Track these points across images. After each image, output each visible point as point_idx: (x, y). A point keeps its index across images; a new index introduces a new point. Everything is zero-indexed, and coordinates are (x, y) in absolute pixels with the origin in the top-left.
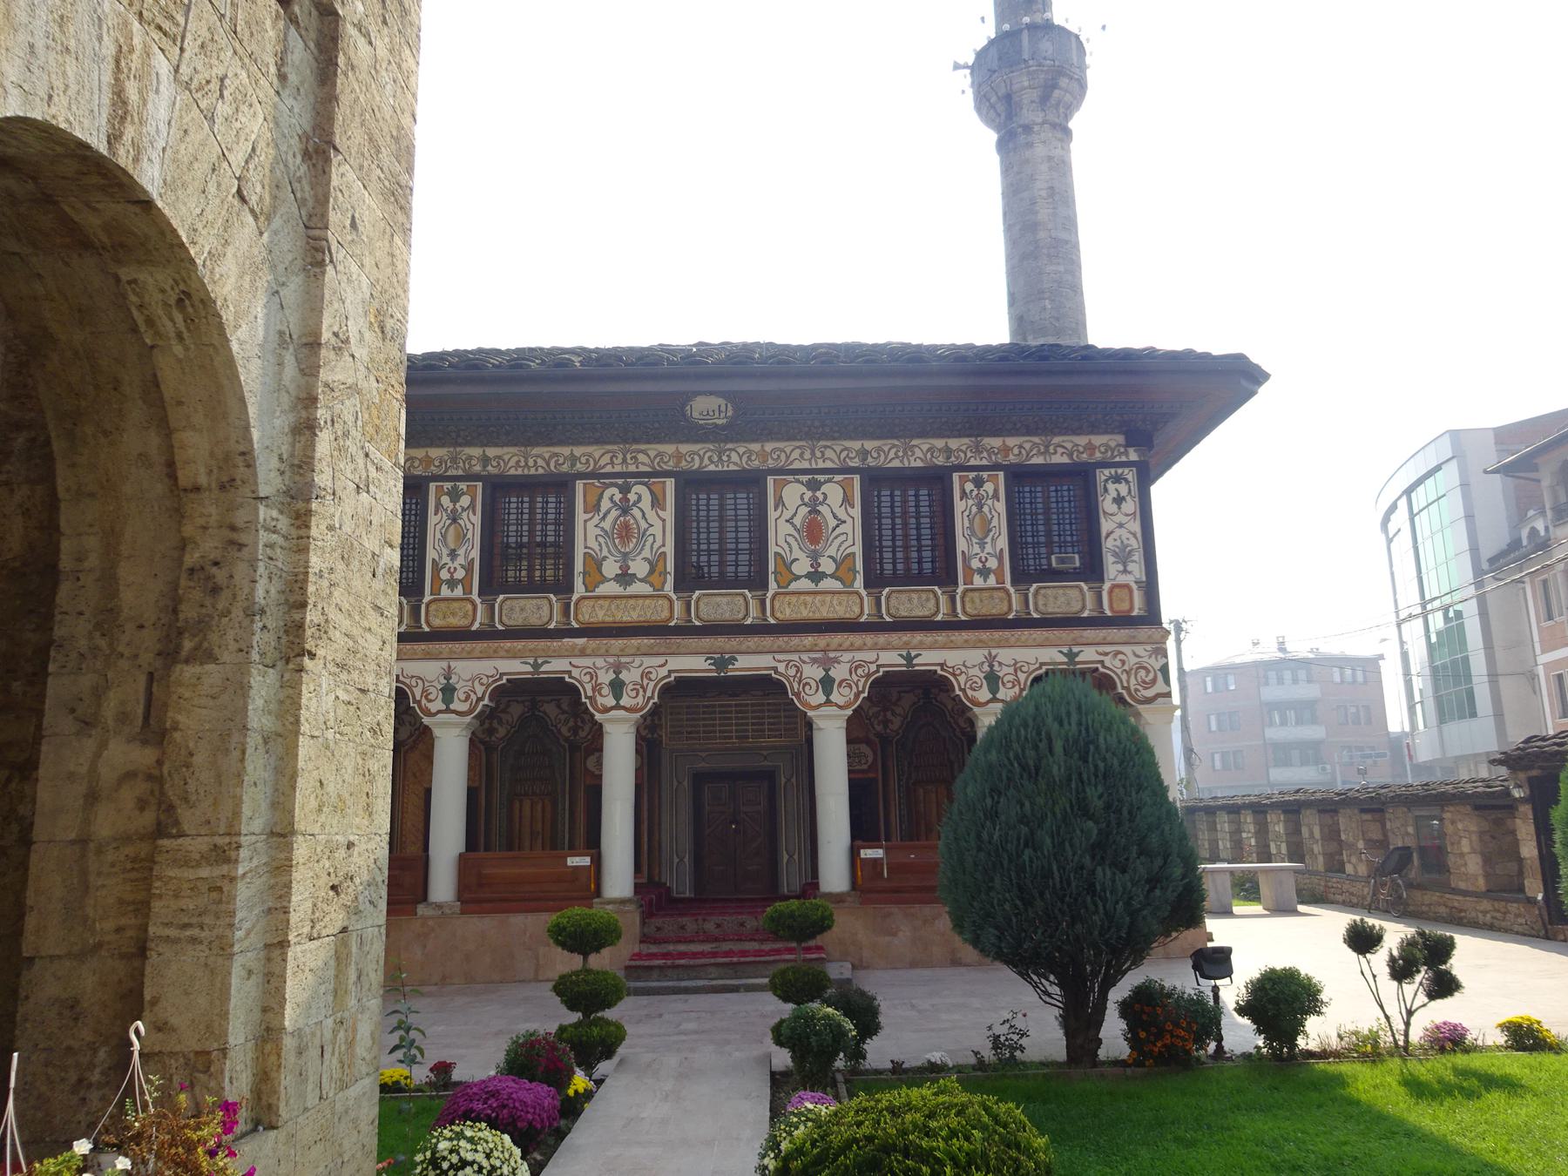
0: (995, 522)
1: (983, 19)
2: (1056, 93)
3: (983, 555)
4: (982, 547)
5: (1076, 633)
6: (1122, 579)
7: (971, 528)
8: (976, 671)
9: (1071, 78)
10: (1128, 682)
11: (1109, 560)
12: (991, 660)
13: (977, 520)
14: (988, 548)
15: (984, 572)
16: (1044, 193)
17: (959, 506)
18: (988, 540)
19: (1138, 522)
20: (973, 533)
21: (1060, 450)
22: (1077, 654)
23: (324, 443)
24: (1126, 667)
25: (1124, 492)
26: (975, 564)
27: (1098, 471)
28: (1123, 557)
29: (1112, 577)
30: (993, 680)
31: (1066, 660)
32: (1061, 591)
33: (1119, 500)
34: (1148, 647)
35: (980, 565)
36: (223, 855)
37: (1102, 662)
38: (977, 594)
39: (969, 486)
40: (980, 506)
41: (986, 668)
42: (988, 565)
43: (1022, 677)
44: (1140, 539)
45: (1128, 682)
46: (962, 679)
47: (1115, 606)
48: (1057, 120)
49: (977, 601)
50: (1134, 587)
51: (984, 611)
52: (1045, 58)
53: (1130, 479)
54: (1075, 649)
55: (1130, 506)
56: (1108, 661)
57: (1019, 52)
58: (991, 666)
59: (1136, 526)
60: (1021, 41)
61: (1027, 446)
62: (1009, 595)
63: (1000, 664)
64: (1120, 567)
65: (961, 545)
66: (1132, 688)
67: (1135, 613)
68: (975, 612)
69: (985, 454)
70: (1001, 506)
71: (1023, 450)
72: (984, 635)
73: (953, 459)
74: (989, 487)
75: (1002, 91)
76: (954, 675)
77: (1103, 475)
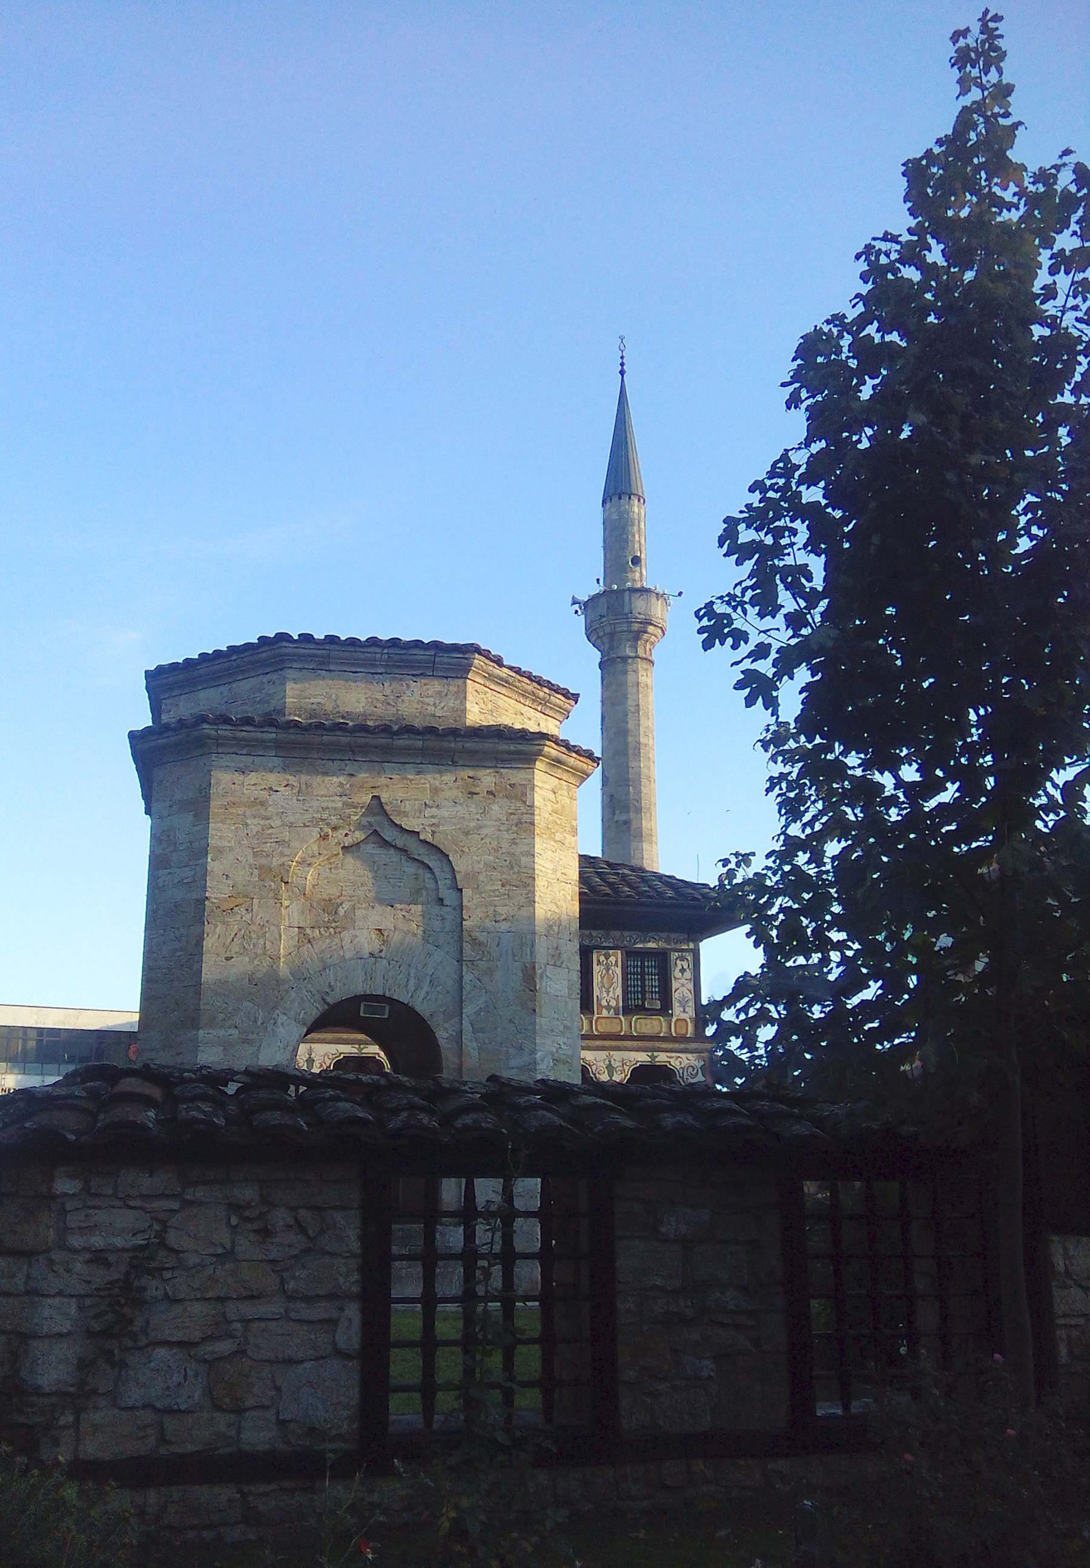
0: (615, 980)
1: (598, 580)
2: (645, 636)
3: (608, 998)
4: (608, 992)
5: (657, 1044)
6: (683, 1016)
7: (602, 982)
8: (601, 1064)
9: (655, 626)
10: (683, 1073)
11: (676, 1004)
12: (609, 1057)
13: (605, 979)
14: (611, 994)
15: (608, 1008)
16: (632, 709)
17: (596, 968)
18: (611, 990)
19: (692, 983)
20: (603, 986)
21: (653, 940)
22: (656, 1057)
24: (682, 1066)
25: (686, 967)
26: (604, 1003)
27: (672, 953)
28: (683, 1004)
29: (677, 1014)
30: (610, 1068)
31: (650, 1060)
32: (649, 1021)
33: (683, 970)
34: (694, 1055)
35: (606, 1004)
37: (669, 1062)
38: (603, 1020)
39: (602, 958)
40: (608, 970)
41: (607, 1062)
42: (610, 1004)
43: (626, 1068)
44: (692, 992)
45: (683, 1073)
46: (594, 1068)
47: (678, 1031)
48: (644, 656)
49: (604, 1025)
50: (689, 1021)
51: (607, 1031)
52: (639, 613)
53: (689, 958)
54: (655, 1054)
55: (688, 974)
56: (672, 1061)
57: (623, 606)
58: (610, 1061)
59: (691, 986)
60: (623, 598)
61: (634, 937)
62: (621, 1022)
63: (615, 1060)
64: (682, 1009)
65: (596, 992)
66: (685, 1077)
67: (688, 1036)
68: (603, 1031)
69: (611, 940)
70: (619, 971)
71: (632, 940)
72: (607, 1043)
73: (594, 941)
74: (612, 959)
75: (608, 630)
76: (589, 1065)
77: (674, 955)
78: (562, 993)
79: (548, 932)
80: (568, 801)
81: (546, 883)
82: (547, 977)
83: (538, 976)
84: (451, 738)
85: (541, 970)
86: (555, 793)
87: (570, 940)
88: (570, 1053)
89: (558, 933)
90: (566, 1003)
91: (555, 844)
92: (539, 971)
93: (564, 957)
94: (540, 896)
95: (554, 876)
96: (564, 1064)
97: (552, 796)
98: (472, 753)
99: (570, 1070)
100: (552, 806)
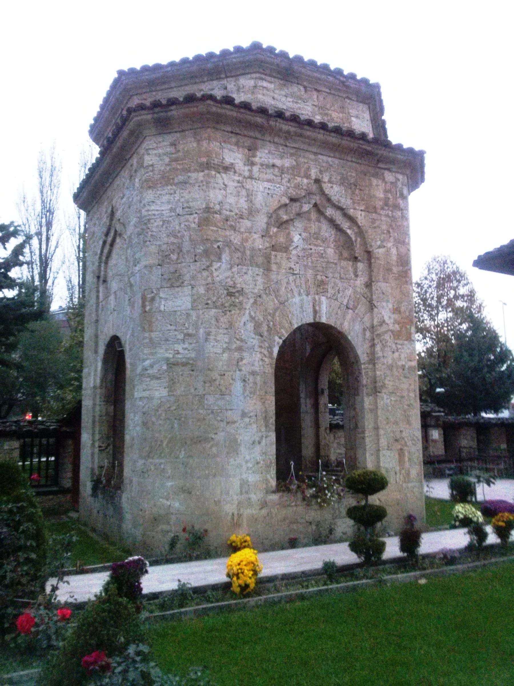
23: (378, 348)
36: (363, 432)
78: (183, 307)
79: (163, 261)
80: (195, 145)
81: (161, 223)
82: (161, 298)
83: (148, 299)
84: (112, 146)
85: (153, 295)
86: (175, 145)
87: (196, 261)
88: (193, 356)
89: (178, 259)
90: (188, 315)
91: (174, 187)
92: (149, 296)
93: (187, 277)
94: (152, 235)
95: (173, 214)
96: (183, 366)
97: (171, 149)
98: (122, 148)
99: (193, 371)
100: (170, 158)
